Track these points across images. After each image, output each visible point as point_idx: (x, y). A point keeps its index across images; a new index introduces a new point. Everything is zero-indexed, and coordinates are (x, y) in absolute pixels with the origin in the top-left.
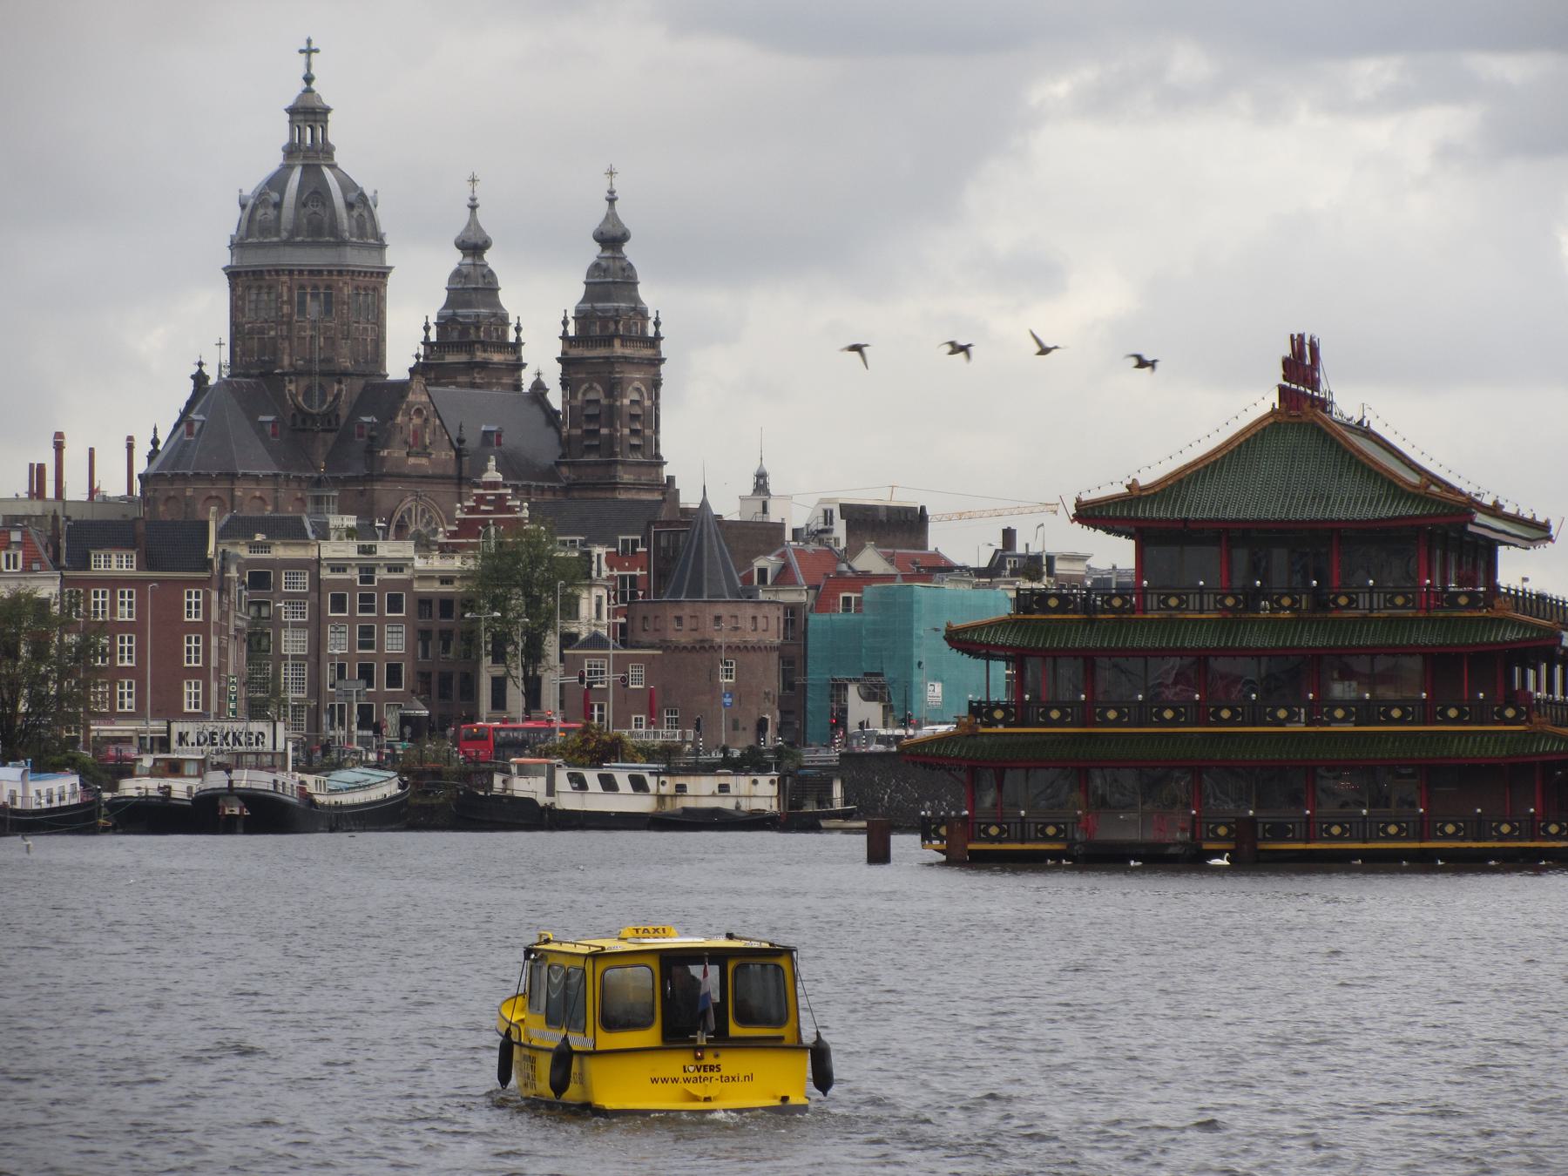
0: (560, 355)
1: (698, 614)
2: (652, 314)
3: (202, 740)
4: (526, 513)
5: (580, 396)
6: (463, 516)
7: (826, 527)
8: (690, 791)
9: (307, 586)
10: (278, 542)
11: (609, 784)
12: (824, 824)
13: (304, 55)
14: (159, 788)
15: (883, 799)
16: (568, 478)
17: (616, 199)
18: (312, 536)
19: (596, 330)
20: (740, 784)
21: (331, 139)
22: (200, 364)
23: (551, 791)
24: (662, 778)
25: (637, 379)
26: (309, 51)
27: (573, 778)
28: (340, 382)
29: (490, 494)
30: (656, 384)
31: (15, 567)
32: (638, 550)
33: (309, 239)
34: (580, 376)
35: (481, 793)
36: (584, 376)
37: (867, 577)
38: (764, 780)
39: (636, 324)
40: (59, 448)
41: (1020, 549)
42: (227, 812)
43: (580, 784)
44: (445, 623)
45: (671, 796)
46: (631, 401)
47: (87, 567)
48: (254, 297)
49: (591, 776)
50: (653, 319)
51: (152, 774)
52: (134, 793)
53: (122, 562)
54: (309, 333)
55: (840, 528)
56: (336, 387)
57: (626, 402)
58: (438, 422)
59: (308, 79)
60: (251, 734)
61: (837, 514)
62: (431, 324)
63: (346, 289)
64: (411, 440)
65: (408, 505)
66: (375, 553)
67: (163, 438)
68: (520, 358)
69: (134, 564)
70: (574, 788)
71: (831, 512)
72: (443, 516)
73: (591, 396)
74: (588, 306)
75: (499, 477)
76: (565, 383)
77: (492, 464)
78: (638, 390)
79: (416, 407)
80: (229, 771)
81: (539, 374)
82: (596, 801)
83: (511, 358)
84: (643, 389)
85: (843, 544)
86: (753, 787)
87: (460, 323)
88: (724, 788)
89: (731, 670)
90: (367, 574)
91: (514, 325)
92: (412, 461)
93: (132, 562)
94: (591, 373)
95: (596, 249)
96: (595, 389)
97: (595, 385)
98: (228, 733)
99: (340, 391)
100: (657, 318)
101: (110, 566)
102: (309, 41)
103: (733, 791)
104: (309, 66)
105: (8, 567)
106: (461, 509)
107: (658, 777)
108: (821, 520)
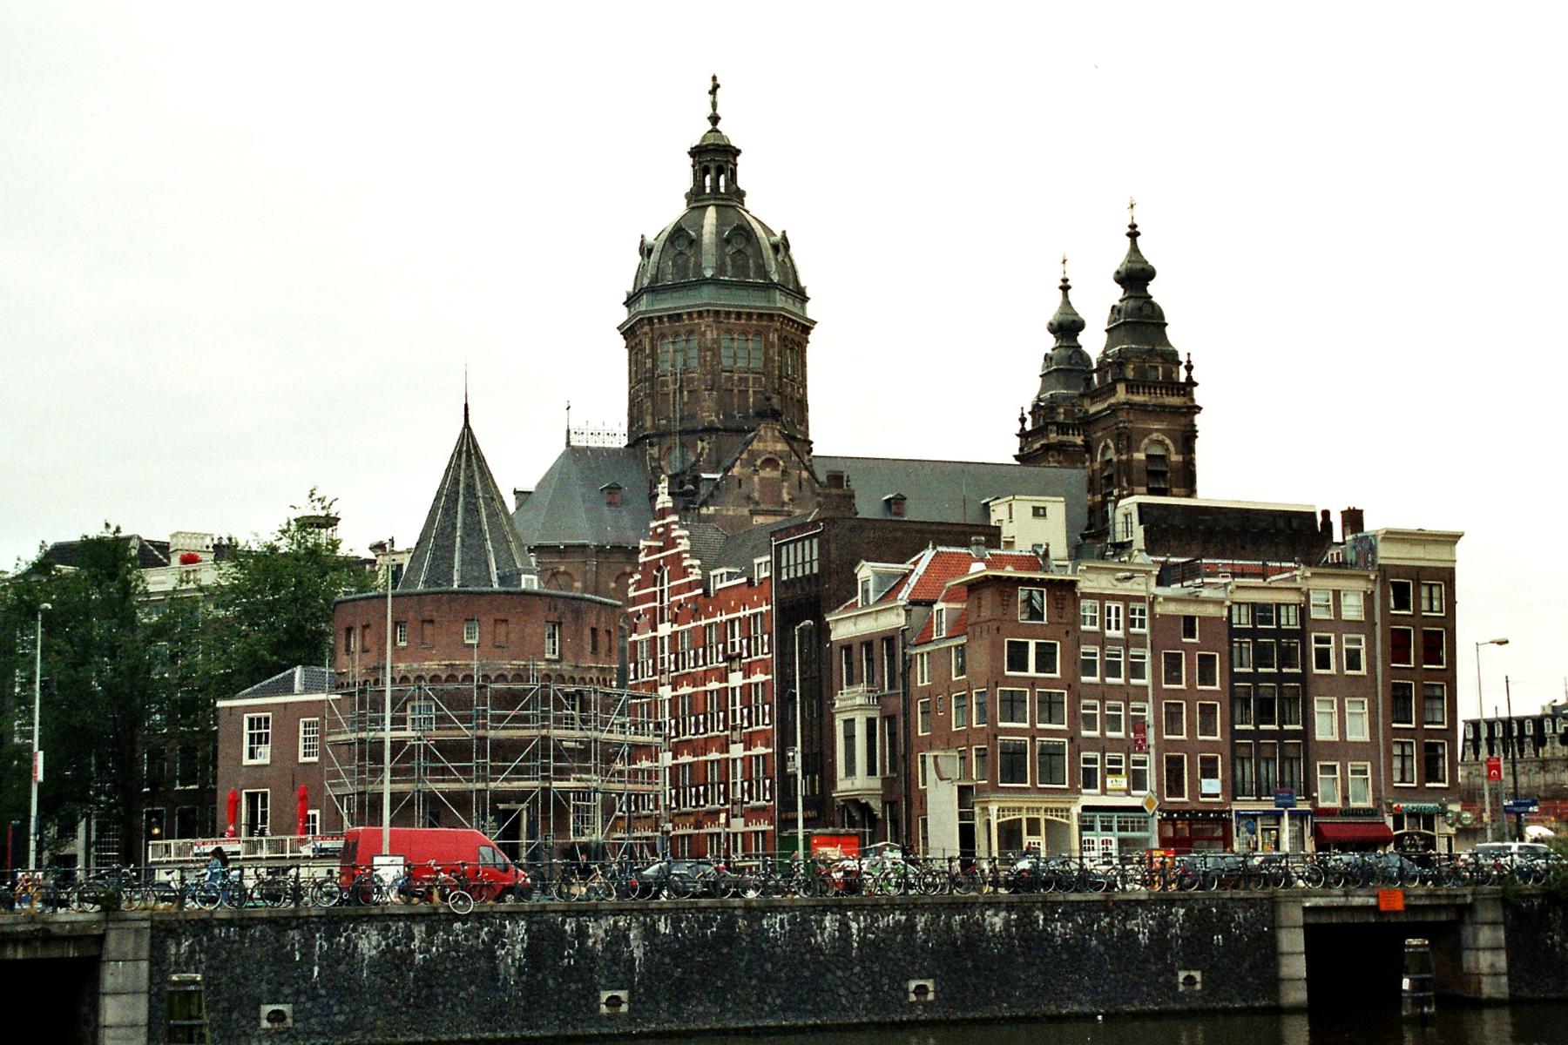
2: (1183, 358)
17: (1138, 234)
25: (1157, 430)
28: (702, 441)
36: (1099, 434)
46: (1148, 456)
50: (1185, 363)
57: (1140, 456)
58: (805, 474)
59: (715, 119)
63: (708, 332)
78: (1161, 443)
95: (1118, 292)
99: (703, 448)
100: (1189, 362)
104: (714, 105)
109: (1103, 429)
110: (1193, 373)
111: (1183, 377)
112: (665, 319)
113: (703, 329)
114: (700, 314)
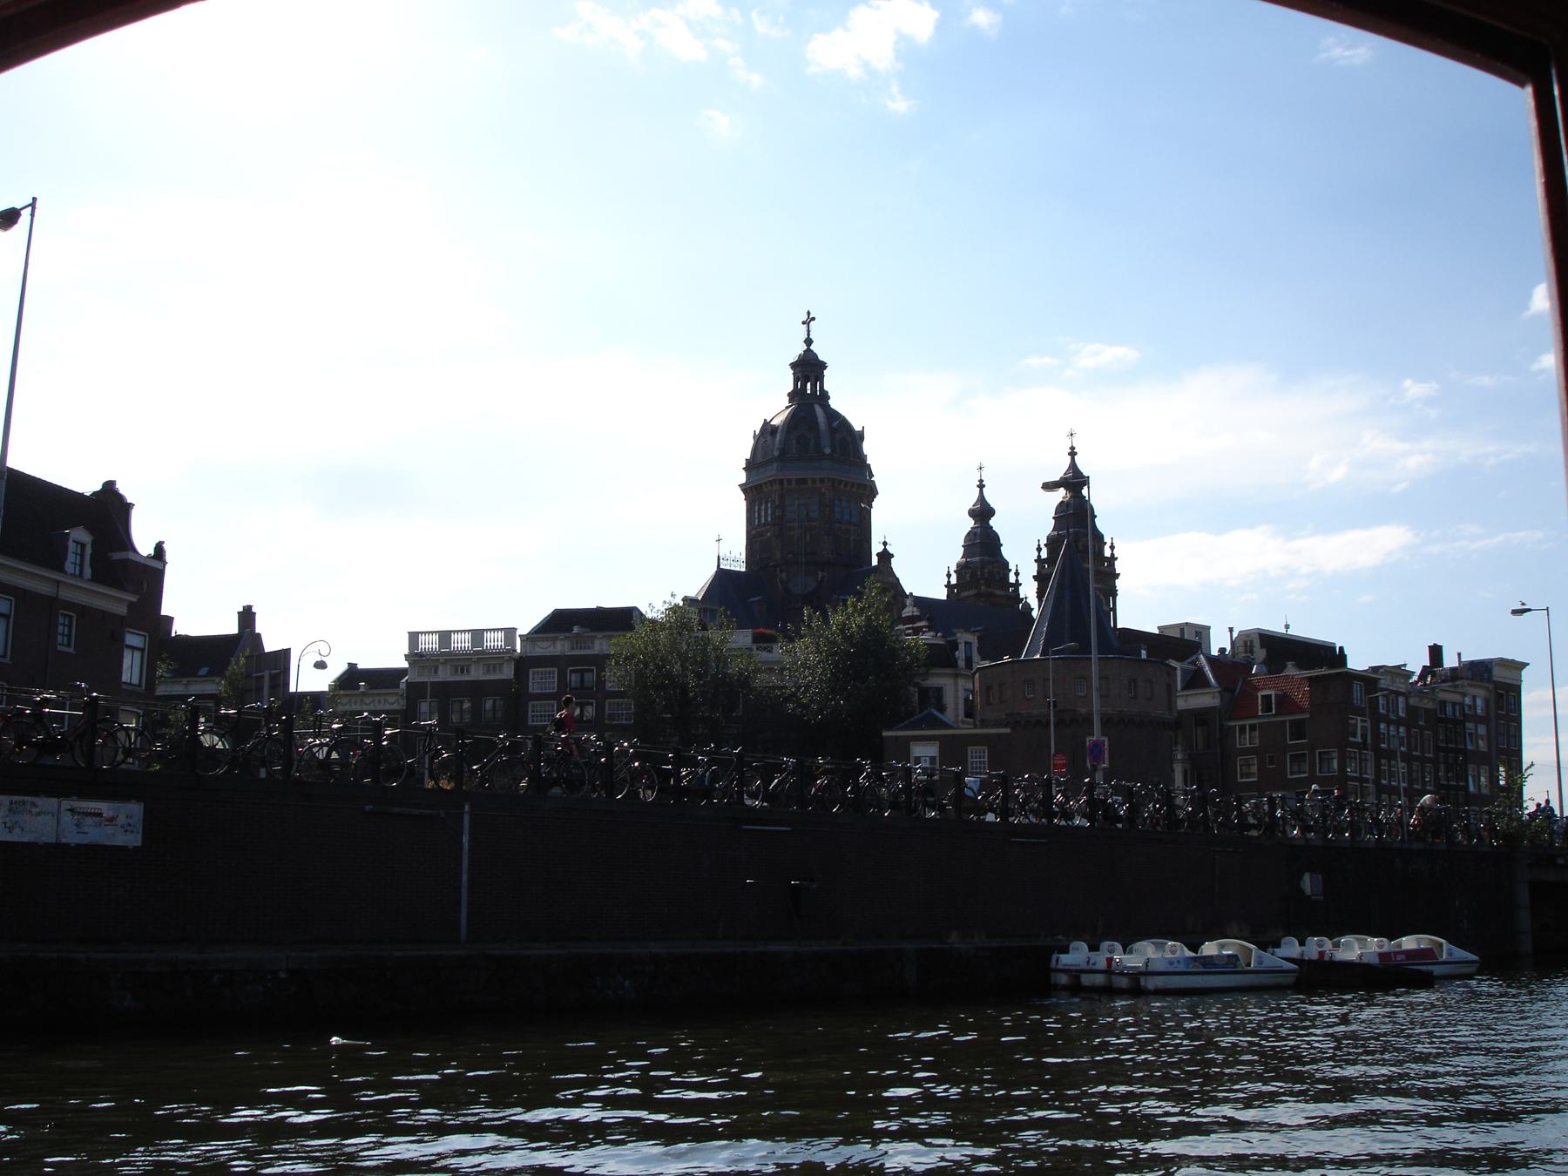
0: (1036, 574)
10: (600, 635)
13: (805, 326)
17: (1076, 454)
21: (826, 388)
26: (809, 321)
28: (822, 571)
41: (1450, 662)
48: (757, 508)
55: (1260, 654)
56: (820, 574)
59: (809, 342)
61: (1257, 643)
62: (952, 572)
71: (1251, 641)
74: (1056, 533)
91: (1014, 571)
99: (823, 577)
100: (1112, 543)
102: (809, 313)
110: (1115, 552)
112: (794, 482)
113: (823, 490)
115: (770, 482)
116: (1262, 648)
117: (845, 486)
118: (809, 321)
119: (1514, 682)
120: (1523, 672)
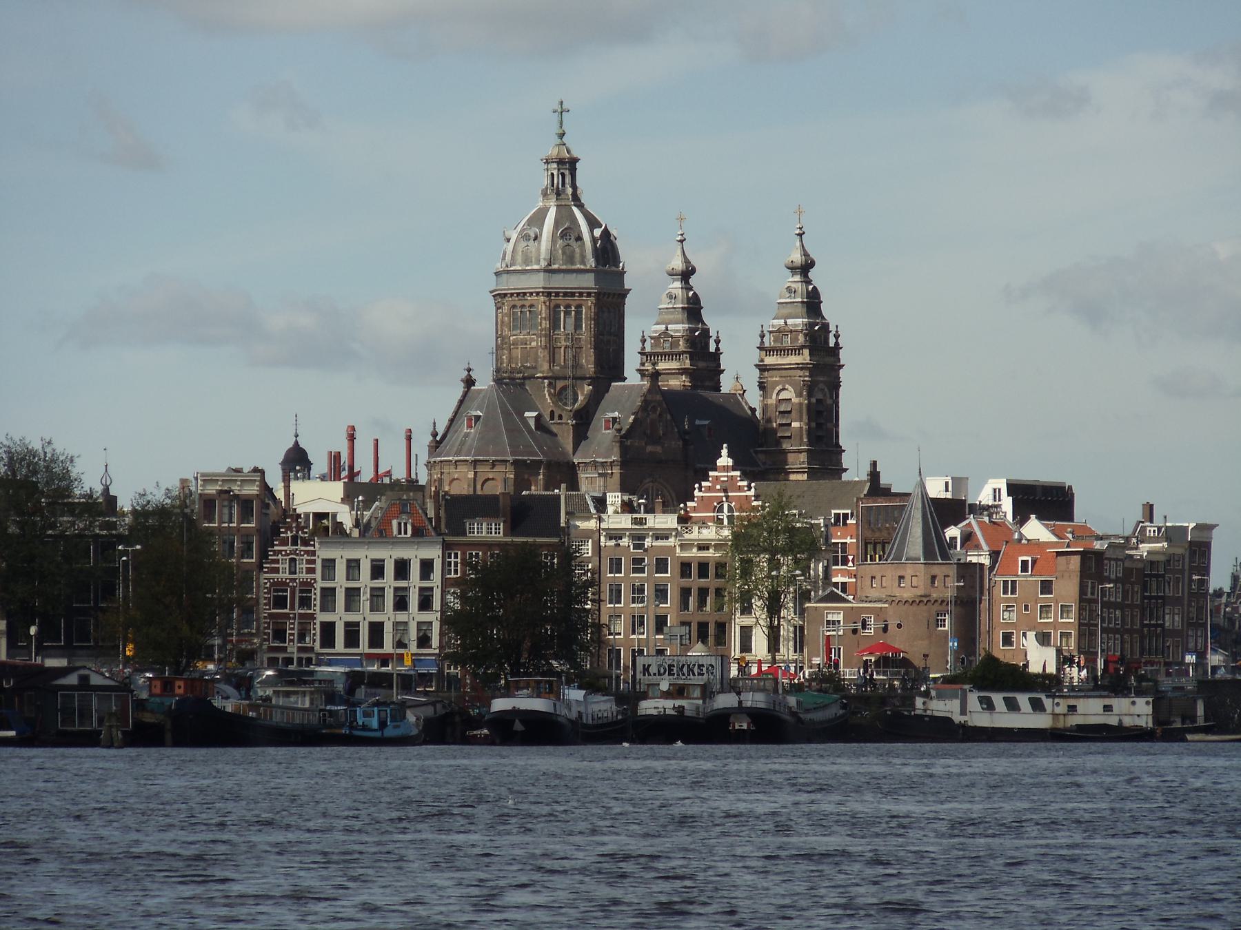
1: (918, 574)
2: (832, 328)
3: (662, 671)
4: (752, 492)
5: (774, 396)
6: (701, 494)
7: (996, 503)
8: (1080, 710)
9: (590, 551)
11: (1012, 706)
12: (1189, 737)
14: (674, 708)
15: (1234, 717)
16: (764, 463)
18: (593, 510)
19: (788, 342)
20: (1121, 704)
22: (469, 370)
23: (963, 711)
24: (1057, 700)
25: (822, 382)
26: (562, 111)
27: (982, 700)
29: (724, 477)
30: (835, 385)
31: (406, 533)
32: (848, 522)
33: (564, 267)
34: (774, 379)
35: (906, 713)
36: (777, 379)
37: (1035, 545)
38: (1141, 701)
39: (820, 336)
40: (352, 438)
41: (1158, 520)
42: (737, 727)
43: (989, 705)
44: (703, 582)
45: (1064, 715)
46: (817, 400)
47: (464, 534)
49: (998, 698)
50: (833, 332)
51: (667, 695)
52: (655, 712)
53: (491, 529)
54: (564, 343)
55: (1007, 504)
57: (814, 400)
58: (669, 417)
60: (703, 666)
64: (649, 432)
65: (646, 486)
66: (646, 524)
67: (441, 430)
68: (719, 365)
69: (501, 531)
70: (983, 709)
71: (1000, 490)
72: (674, 495)
73: (783, 395)
75: (730, 462)
76: (762, 386)
77: (724, 452)
79: (652, 405)
80: (739, 693)
81: (737, 378)
82: (1003, 719)
83: (712, 365)
84: (826, 390)
85: (1010, 517)
86: (1131, 706)
87: (672, 337)
88: (1108, 708)
89: (945, 620)
90: (638, 539)
92: (649, 449)
93: (499, 529)
94: (785, 377)
96: (787, 389)
97: (787, 386)
98: (683, 666)
100: (837, 332)
101: (482, 533)
102: (562, 103)
103: (1116, 710)
104: (561, 123)
105: (400, 533)
106: (700, 490)
107: (1053, 699)
108: (991, 497)
109: (781, 377)
111: (832, 344)
114: (589, 295)
115: (538, 293)
116: (1008, 496)
117: (608, 298)
118: (562, 111)
119: (1205, 540)
120: (1214, 531)
